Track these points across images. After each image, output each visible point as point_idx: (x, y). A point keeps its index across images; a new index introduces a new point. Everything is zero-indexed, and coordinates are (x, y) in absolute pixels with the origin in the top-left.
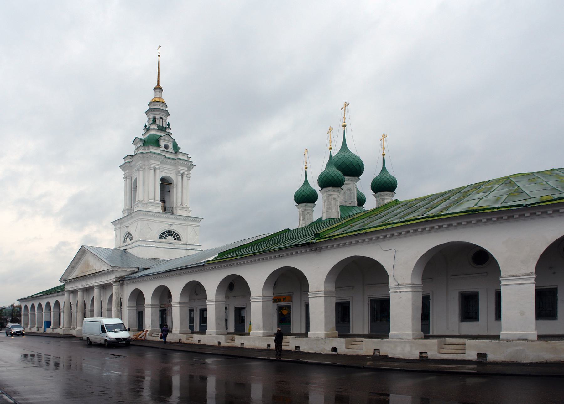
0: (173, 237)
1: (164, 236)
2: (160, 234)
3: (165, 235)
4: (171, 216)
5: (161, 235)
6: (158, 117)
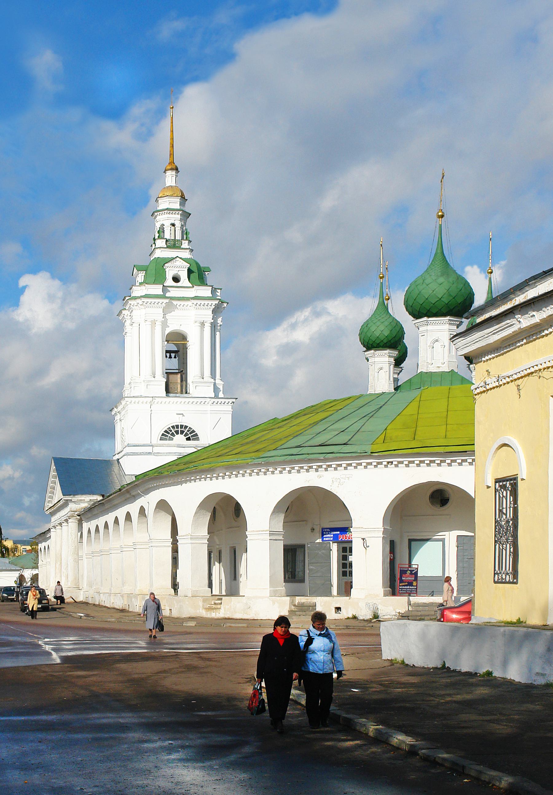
0: (185, 436)
1: (169, 435)
3: (171, 433)
4: (187, 400)
5: (163, 435)
6: (167, 224)
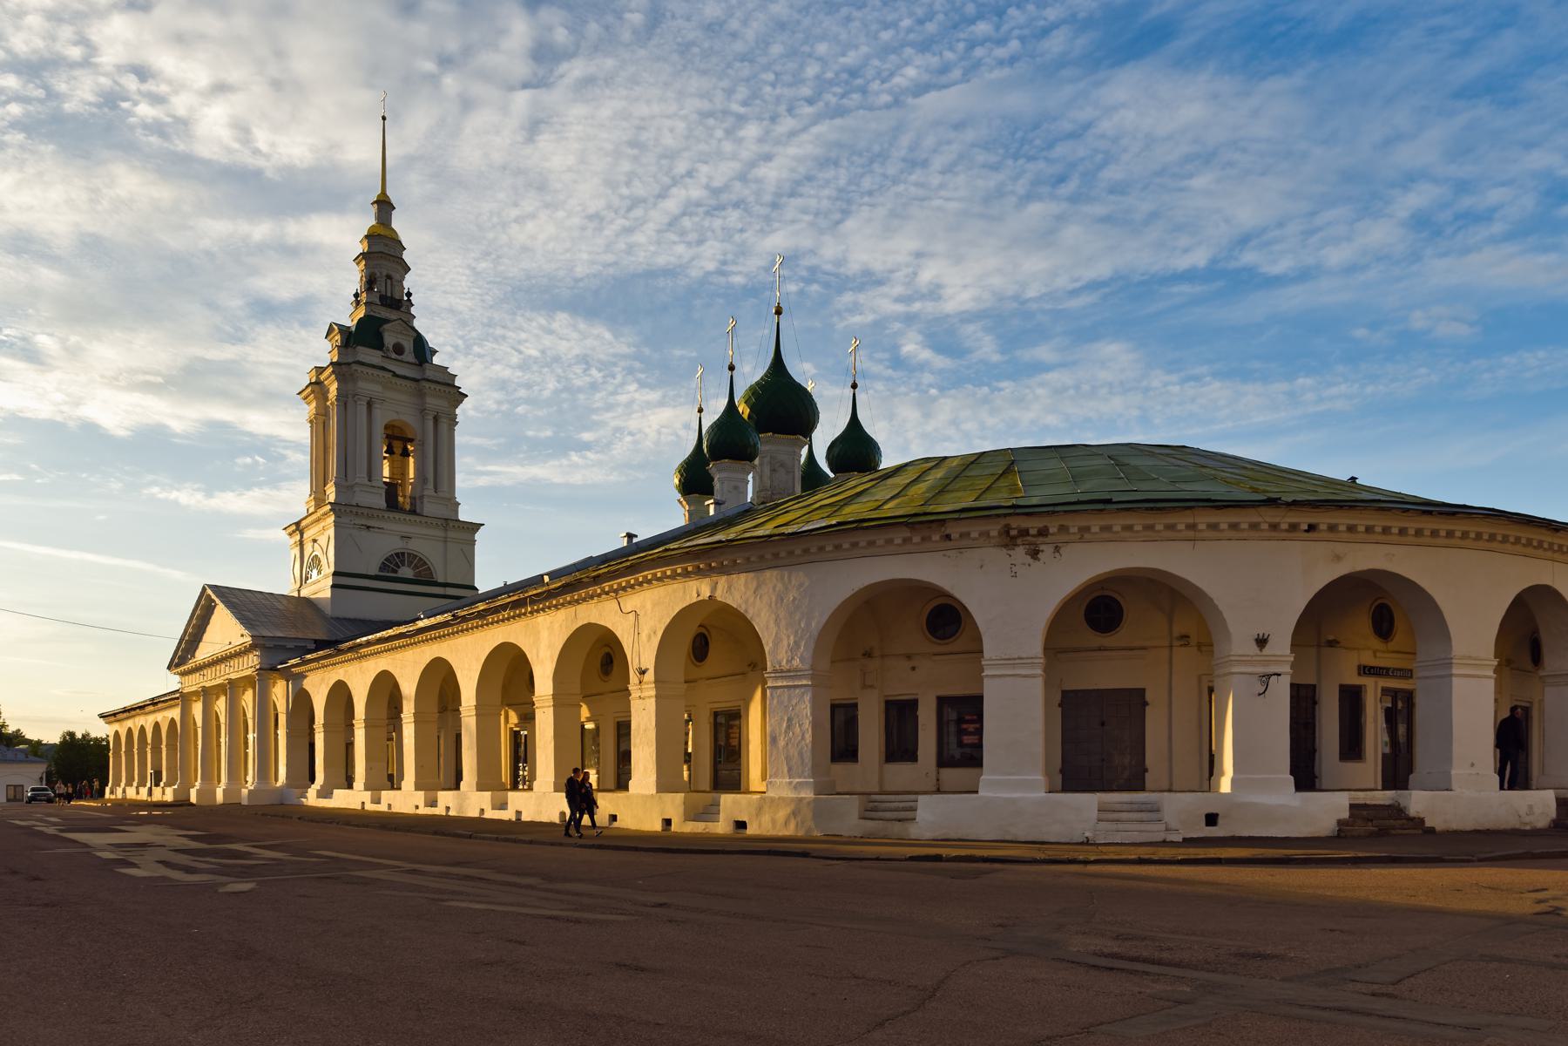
2: (382, 560)
